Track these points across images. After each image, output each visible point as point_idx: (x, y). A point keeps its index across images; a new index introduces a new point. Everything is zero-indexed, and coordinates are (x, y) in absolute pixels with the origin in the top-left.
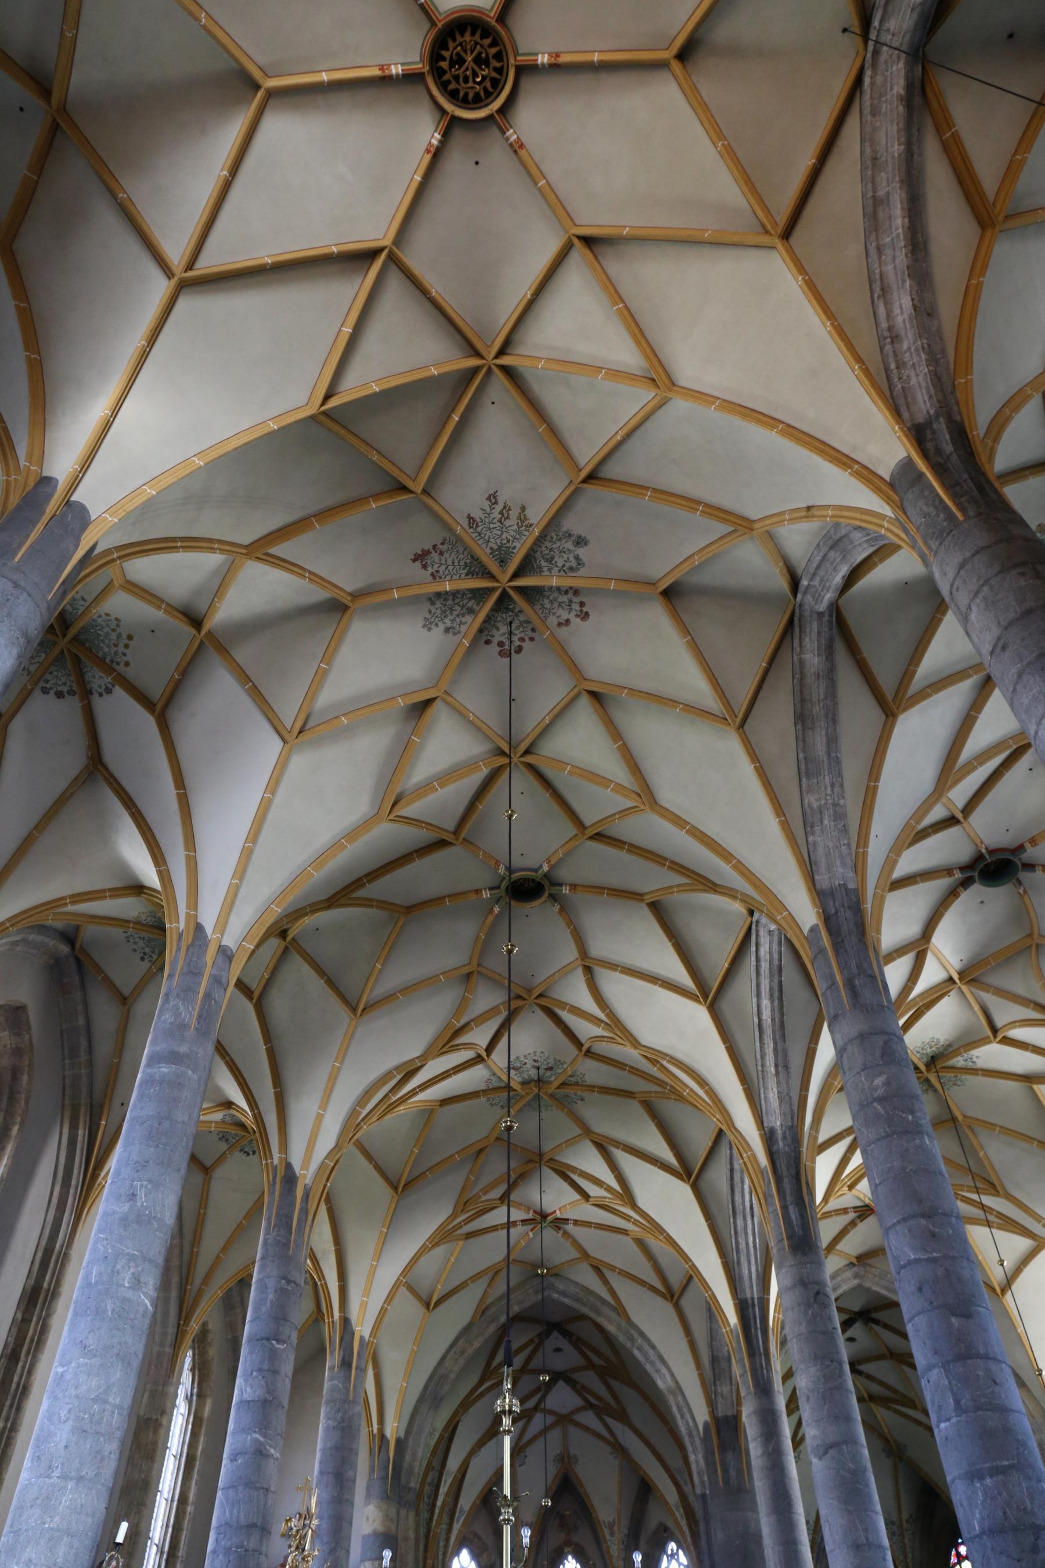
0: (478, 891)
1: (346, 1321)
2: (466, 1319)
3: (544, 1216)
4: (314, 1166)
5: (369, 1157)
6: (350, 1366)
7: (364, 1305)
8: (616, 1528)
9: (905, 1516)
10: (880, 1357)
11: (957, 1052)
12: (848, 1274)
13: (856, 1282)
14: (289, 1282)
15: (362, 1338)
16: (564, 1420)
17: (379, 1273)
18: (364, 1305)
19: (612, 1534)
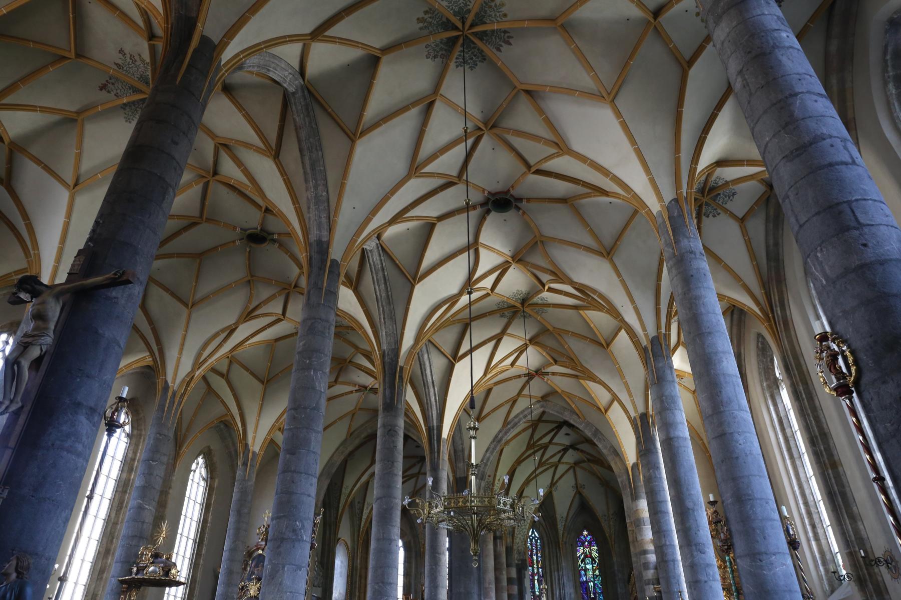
0: (234, 242)
1: (246, 445)
2: (344, 437)
3: (366, 388)
4: (178, 381)
5: (247, 369)
6: (246, 465)
7: (254, 438)
9: (611, 512)
10: (582, 442)
11: (533, 297)
12: (538, 405)
13: (542, 410)
14: (160, 435)
15: (254, 453)
17: (261, 422)
18: (254, 438)
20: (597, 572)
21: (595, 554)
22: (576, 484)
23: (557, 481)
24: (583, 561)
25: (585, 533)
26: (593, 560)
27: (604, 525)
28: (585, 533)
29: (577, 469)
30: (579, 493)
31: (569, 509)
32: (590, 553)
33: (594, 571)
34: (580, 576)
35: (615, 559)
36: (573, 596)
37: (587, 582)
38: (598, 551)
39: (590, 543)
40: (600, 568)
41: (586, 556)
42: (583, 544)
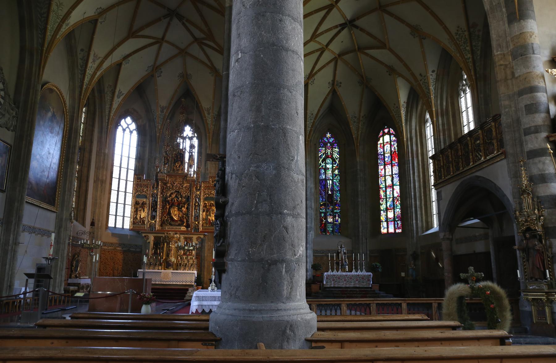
8: (211, 111)
9: (362, 114)
16: (183, 52)
19: (209, 114)
20: (336, 172)
21: (336, 155)
22: (334, 80)
23: (316, 73)
24: (324, 160)
25: (328, 135)
26: (334, 160)
27: (353, 127)
28: (328, 135)
29: (339, 62)
30: (334, 92)
31: (321, 107)
32: (332, 154)
33: (333, 171)
34: (320, 174)
35: (358, 160)
36: (313, 190)
37: (326, 180)
38: (339, 153)
39: (332, 145)
40: (339, 168)
41: (327, 157)
42: (325, 145)
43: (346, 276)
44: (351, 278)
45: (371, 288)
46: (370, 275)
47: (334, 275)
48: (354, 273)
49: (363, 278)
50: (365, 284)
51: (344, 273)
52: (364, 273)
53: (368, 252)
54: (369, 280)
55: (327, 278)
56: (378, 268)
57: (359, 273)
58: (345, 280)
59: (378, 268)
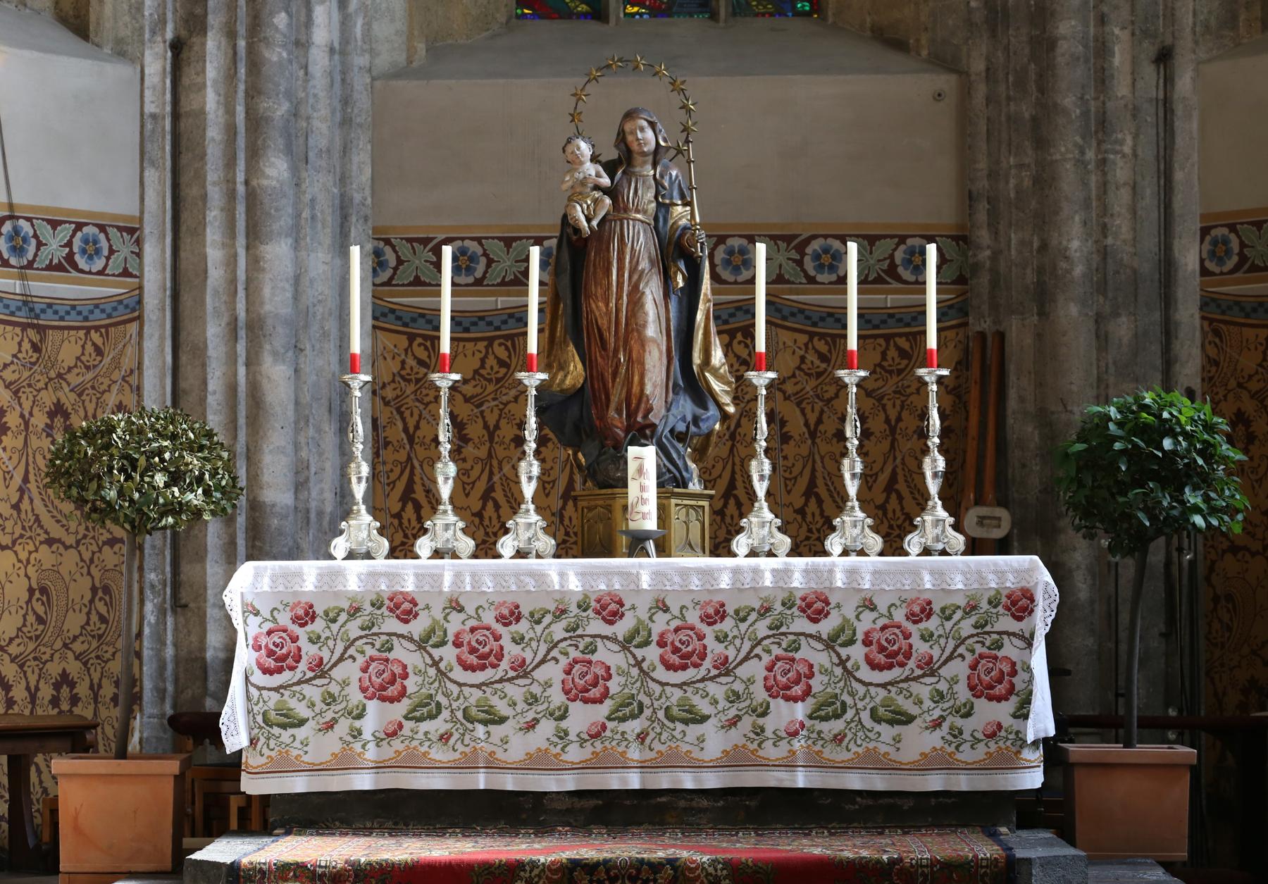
43: (610, 609)
44: (888, 654)
45: (1027, 810)
46: (1021, 604)
47: (404, 608)
48: (760, 560)
49: (888, 654)
50: (919, 741)
51: (571, 576)
52: (943, 564)
53: (1189, 257)
54: (1003, 684)
55: (278, 659)
56: (1175, 475)
57: (851, 561)
58: (587, 688)
59: (1175, 475)
